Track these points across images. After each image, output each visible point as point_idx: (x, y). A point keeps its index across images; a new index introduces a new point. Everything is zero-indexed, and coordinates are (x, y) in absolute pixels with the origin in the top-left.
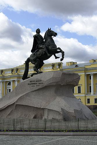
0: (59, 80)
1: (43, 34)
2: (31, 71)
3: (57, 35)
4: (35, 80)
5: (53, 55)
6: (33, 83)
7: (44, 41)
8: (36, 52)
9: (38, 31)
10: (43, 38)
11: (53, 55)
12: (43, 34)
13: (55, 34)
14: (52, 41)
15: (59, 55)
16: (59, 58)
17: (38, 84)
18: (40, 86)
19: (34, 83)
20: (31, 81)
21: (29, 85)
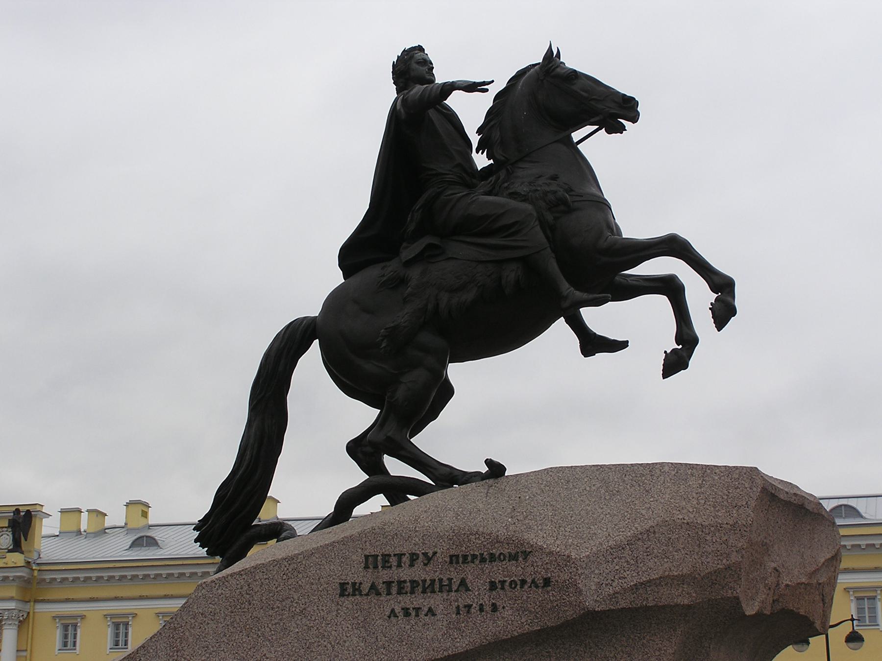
0: (735, 558)
3: (634, 119)
4: (443, 550)
6: (406, 574)
8: (408, 264)
10: (475, 139)
13: (615, 111)
15: (641, 322)
17: (479, 594)
18: (507, 613)
19: (418, 573)
20: (371, 562)
21: (348, 602)
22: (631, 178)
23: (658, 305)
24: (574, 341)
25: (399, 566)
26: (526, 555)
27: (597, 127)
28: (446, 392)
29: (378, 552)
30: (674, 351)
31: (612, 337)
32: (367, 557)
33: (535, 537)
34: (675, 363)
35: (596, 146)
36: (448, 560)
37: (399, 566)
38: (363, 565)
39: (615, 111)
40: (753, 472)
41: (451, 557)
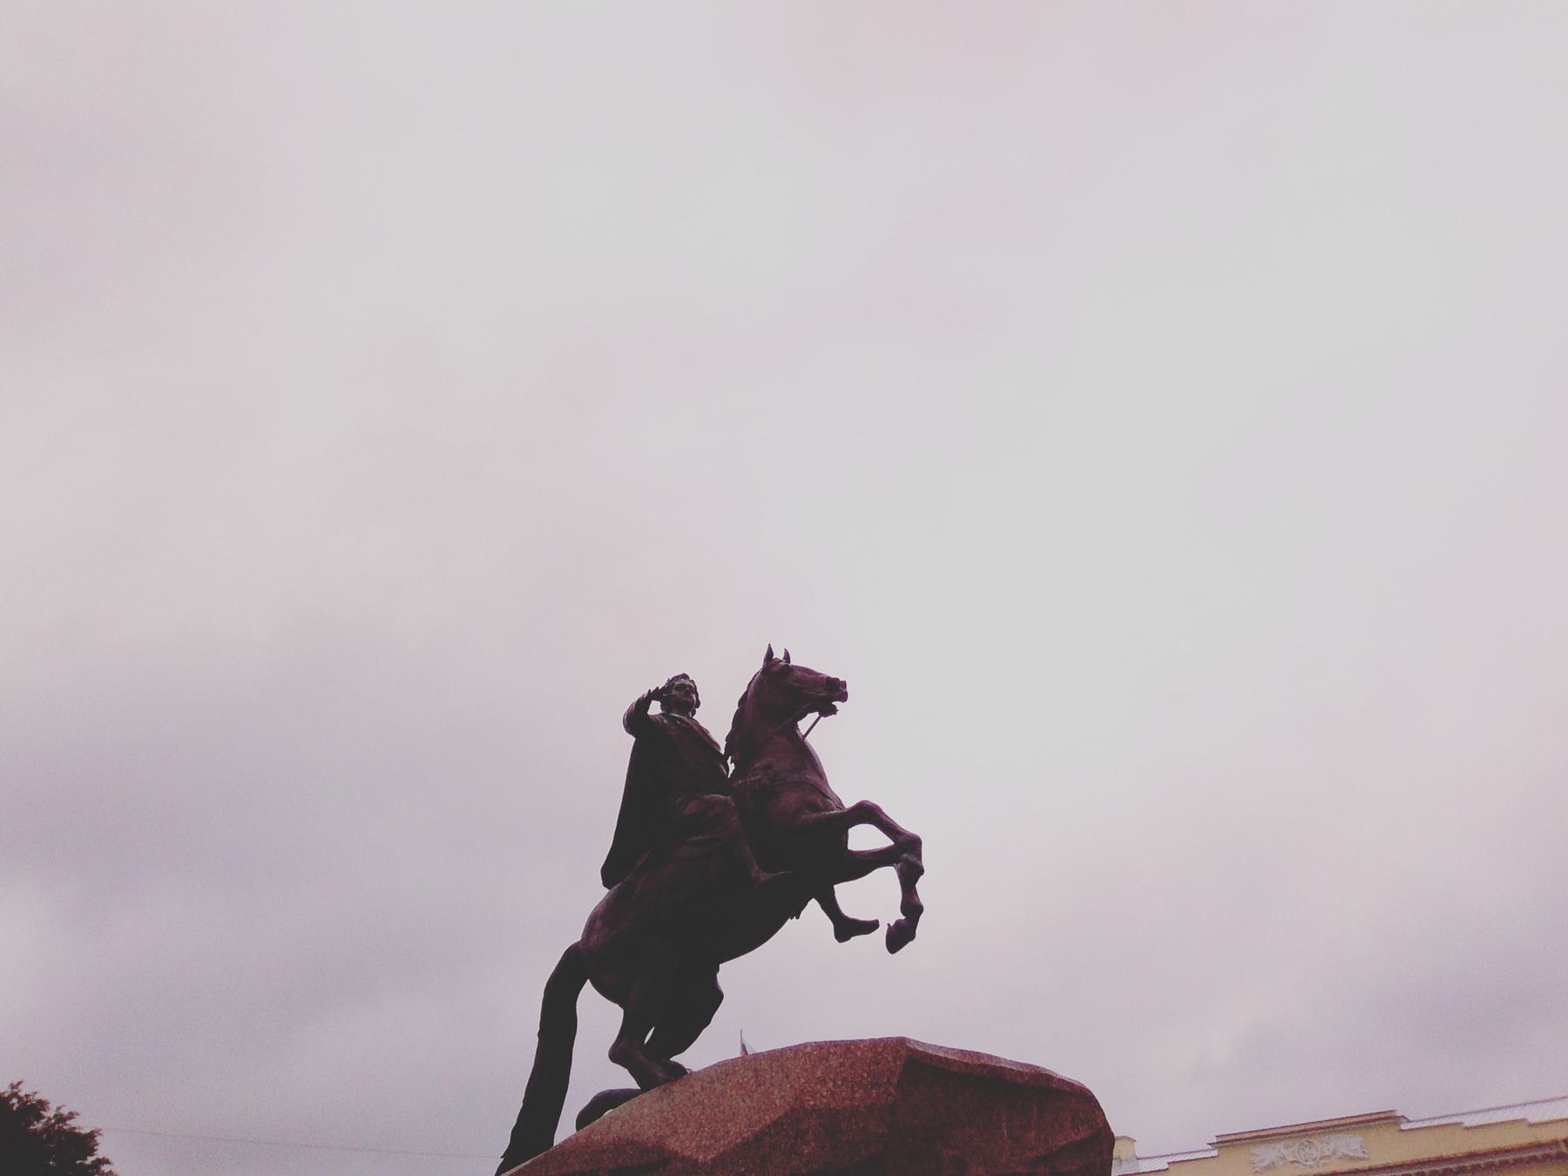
1: (716, 718)
2: (594, 1070)
3: (843, 697)
5: (813, 906)
7: (732, 767)
9: (680, 695)
11: (813, 906)
12: (716, 718)
13: (825, 694)
14: (805, 759)
16: (870, 927)
22: (848, 756)
23: (886, 879)
24: (828, 925)
27: (816, 714)
28: (715, 998)
30: (898, 923)
31: (861, 918)
33: (673, 1144)
34: (900, 936)
35: (818, 733)
39: (825, 694)
40: (899, 1046)
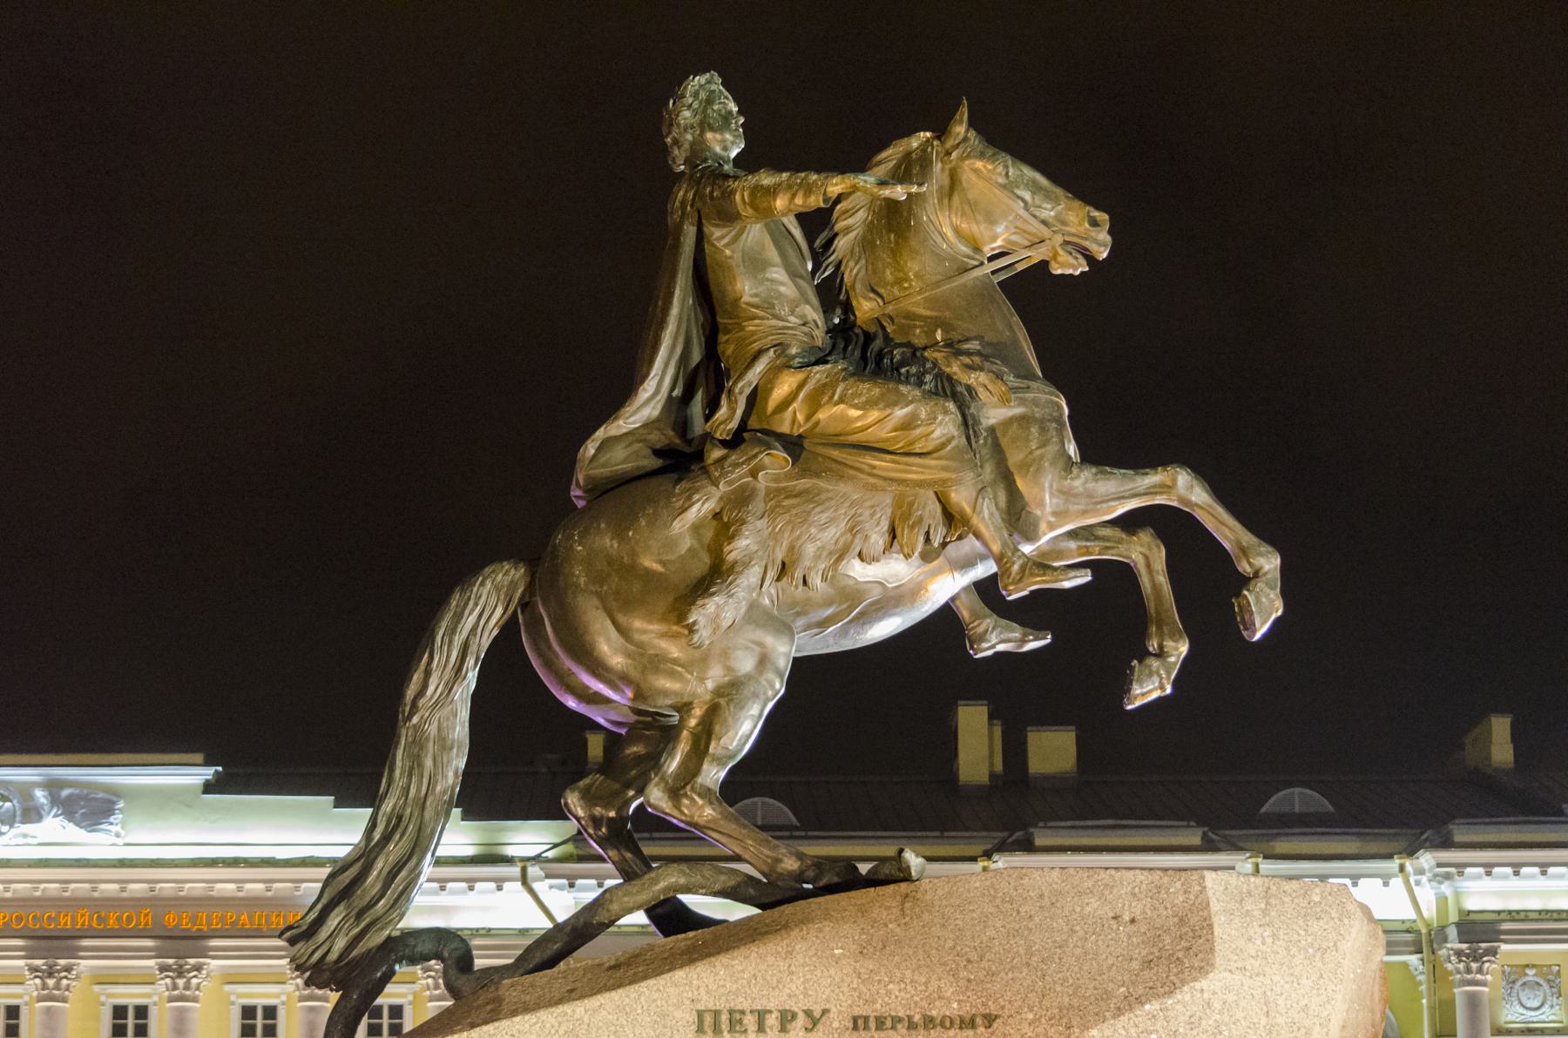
25: (761, 1028)
26: (990, 1020)
29: (722, 1005)
32: (700, 1014)
36: (851, 1025)
37: (761, 1028)
38: (694, 1027)
41: (855, 1020)
